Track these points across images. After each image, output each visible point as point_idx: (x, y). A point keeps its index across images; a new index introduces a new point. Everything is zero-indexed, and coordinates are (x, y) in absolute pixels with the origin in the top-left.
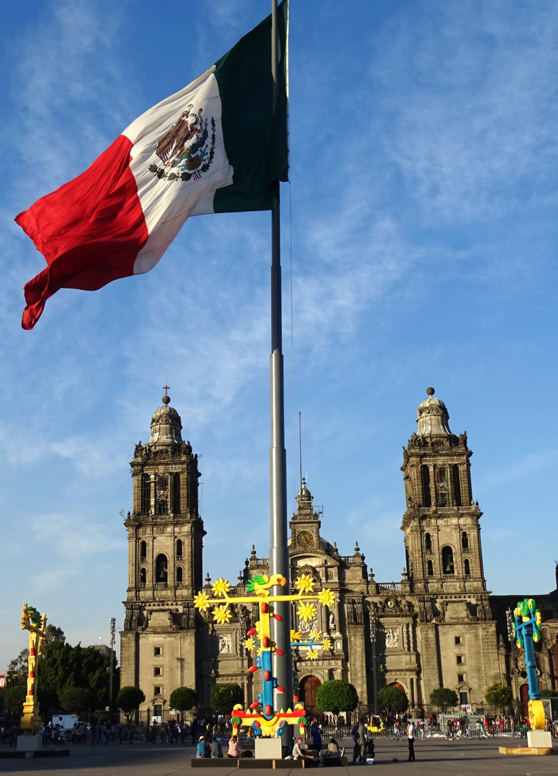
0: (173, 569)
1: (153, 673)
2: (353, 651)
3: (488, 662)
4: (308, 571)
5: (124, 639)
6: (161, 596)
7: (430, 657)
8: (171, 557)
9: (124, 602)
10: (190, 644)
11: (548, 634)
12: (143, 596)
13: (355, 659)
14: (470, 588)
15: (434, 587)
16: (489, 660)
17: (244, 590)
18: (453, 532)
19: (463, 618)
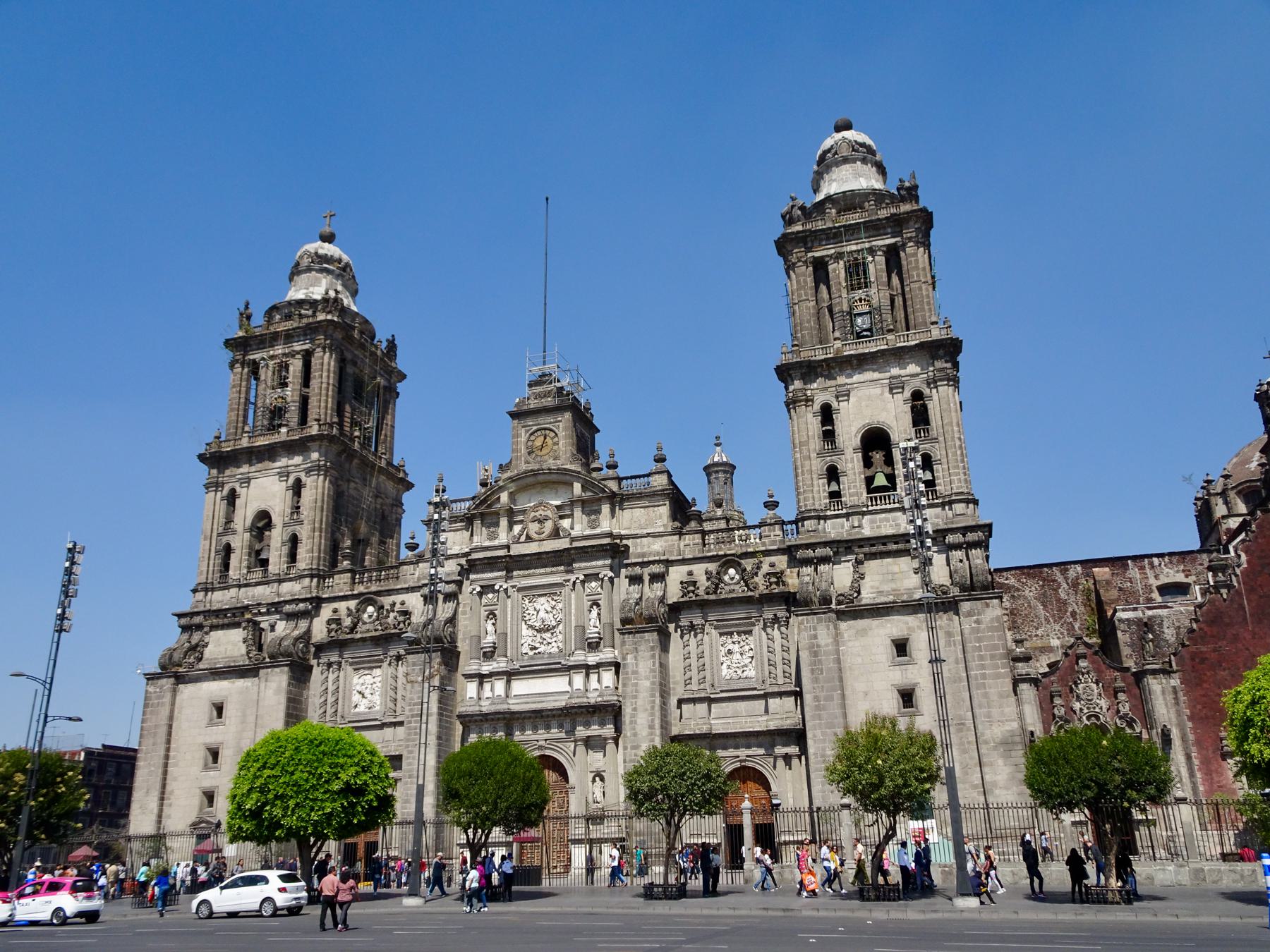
0: (280, 539)
1: (201, 763)
2: (630, 689)
3: (984, 701)
4: (543, 513)
5: (151, 689)
6: (253, 596)
7: (822, 695)
8: (279, 515)
9: (180, 616)
10: (277, 692)
11: (1166, 631)
12: (220, 599)
13: (635, 709)
14: (937, 520)
15: (843, 527)
16: (986, 695)
17: (414, 570)
18: (888, 396)
19: (910, 591)
